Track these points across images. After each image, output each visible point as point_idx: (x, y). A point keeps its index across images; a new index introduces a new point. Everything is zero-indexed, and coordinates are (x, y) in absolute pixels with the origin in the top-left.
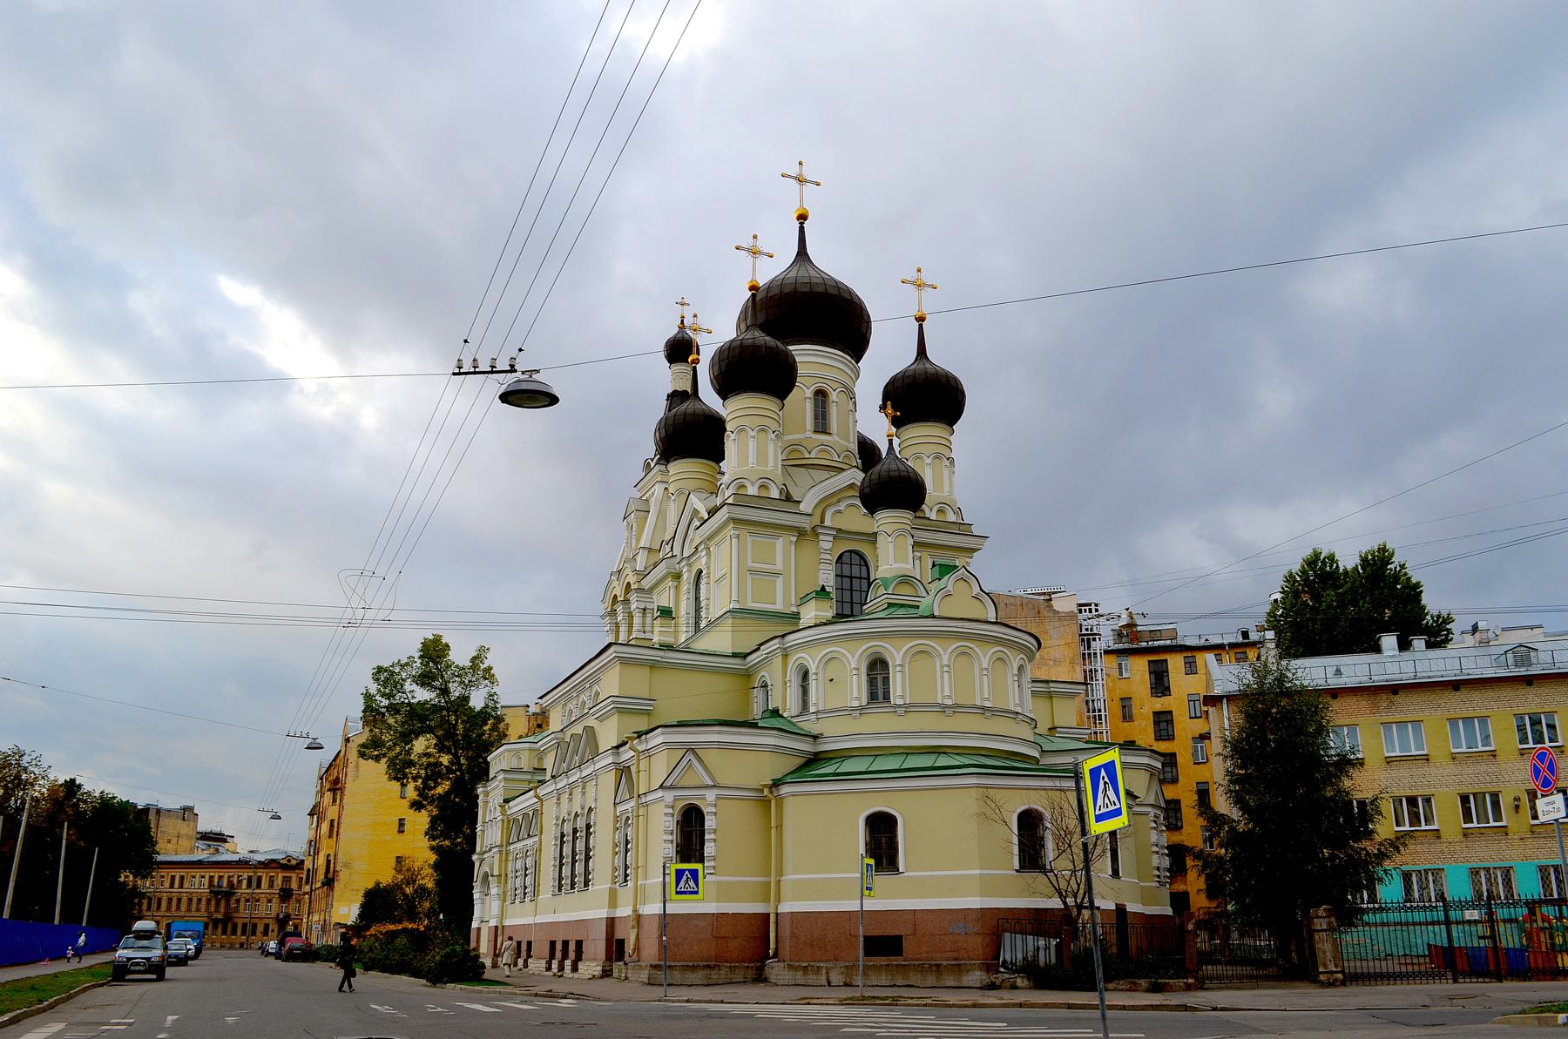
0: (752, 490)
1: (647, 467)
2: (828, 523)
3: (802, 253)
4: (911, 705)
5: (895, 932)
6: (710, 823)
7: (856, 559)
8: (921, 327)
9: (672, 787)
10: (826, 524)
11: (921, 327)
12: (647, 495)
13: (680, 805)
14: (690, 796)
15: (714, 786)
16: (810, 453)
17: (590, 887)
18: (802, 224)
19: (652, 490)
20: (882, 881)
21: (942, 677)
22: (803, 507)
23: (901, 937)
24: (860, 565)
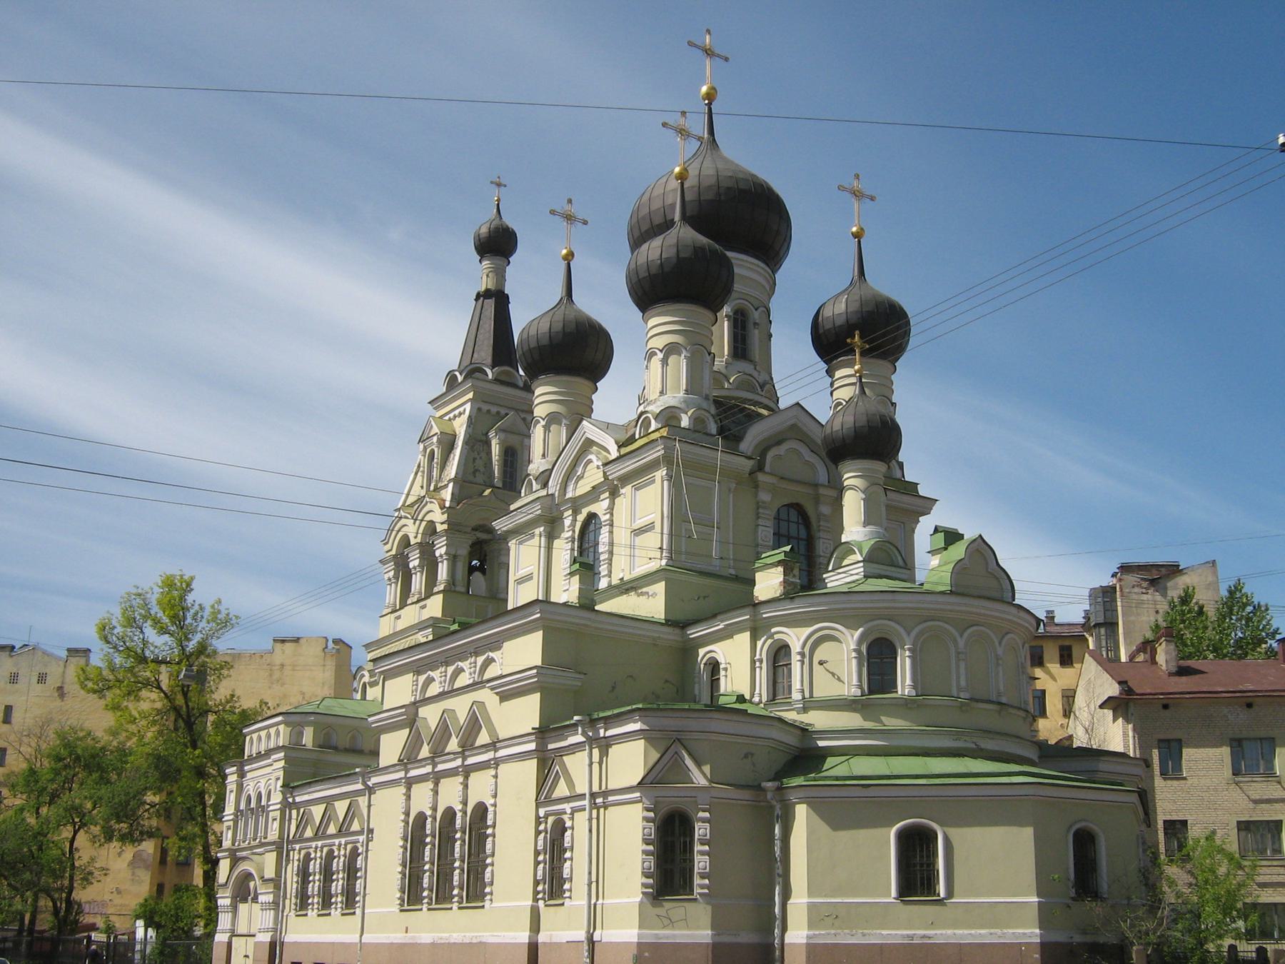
1: (452, 382)
2: (767, 468)
7: (794, 516)
8: (859, 242)
12: (451, 415)
13: (664, 810)
17: (487, 904)
18: (709, 105)
19: (461, 409)
21: (958, 667)
24: (798, 523)
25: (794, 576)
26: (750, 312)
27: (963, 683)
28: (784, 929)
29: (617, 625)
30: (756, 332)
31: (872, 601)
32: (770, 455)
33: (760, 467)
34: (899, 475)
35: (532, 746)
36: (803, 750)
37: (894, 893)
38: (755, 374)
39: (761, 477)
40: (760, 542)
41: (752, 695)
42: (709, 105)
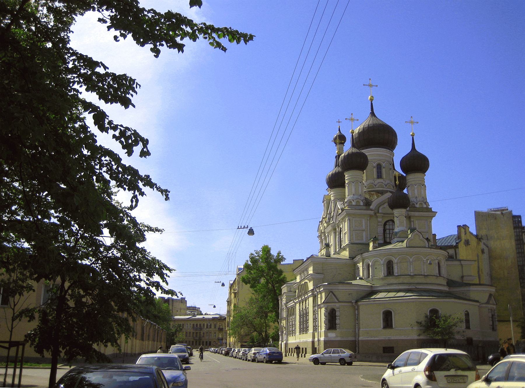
0: (354, 203)
2: (380, 211)
3: (373, 114)
4: (400, 275)
5: (392, 346)
6: (337, 314)
8: (413, 138)
9: (326, 303)
10: (380, 212)
11: (413, 138)
13: (329, 308)
14: (332, 306)
15: (339, 302)
16: (376, 186)
18: (371, 102)
20: (388, 331)
21: (410, 267)
22: (371, 207)
23: (393, 347)
25: (376, 244)
26: (382, 164)
27: (412, 271)
28: (359, 337)
29: (330, 261)
30: (384, 169)
31: (387, 251)
32: (381, 208)
33: (378, 212)
34: (425, 206)
35: (311, 294)
36: (372, 291)
37: (382, 327)
38: (384, 182)
39: (378, 215)
40: (378, 232)
41: (363, 277)
42: (371, 102)
